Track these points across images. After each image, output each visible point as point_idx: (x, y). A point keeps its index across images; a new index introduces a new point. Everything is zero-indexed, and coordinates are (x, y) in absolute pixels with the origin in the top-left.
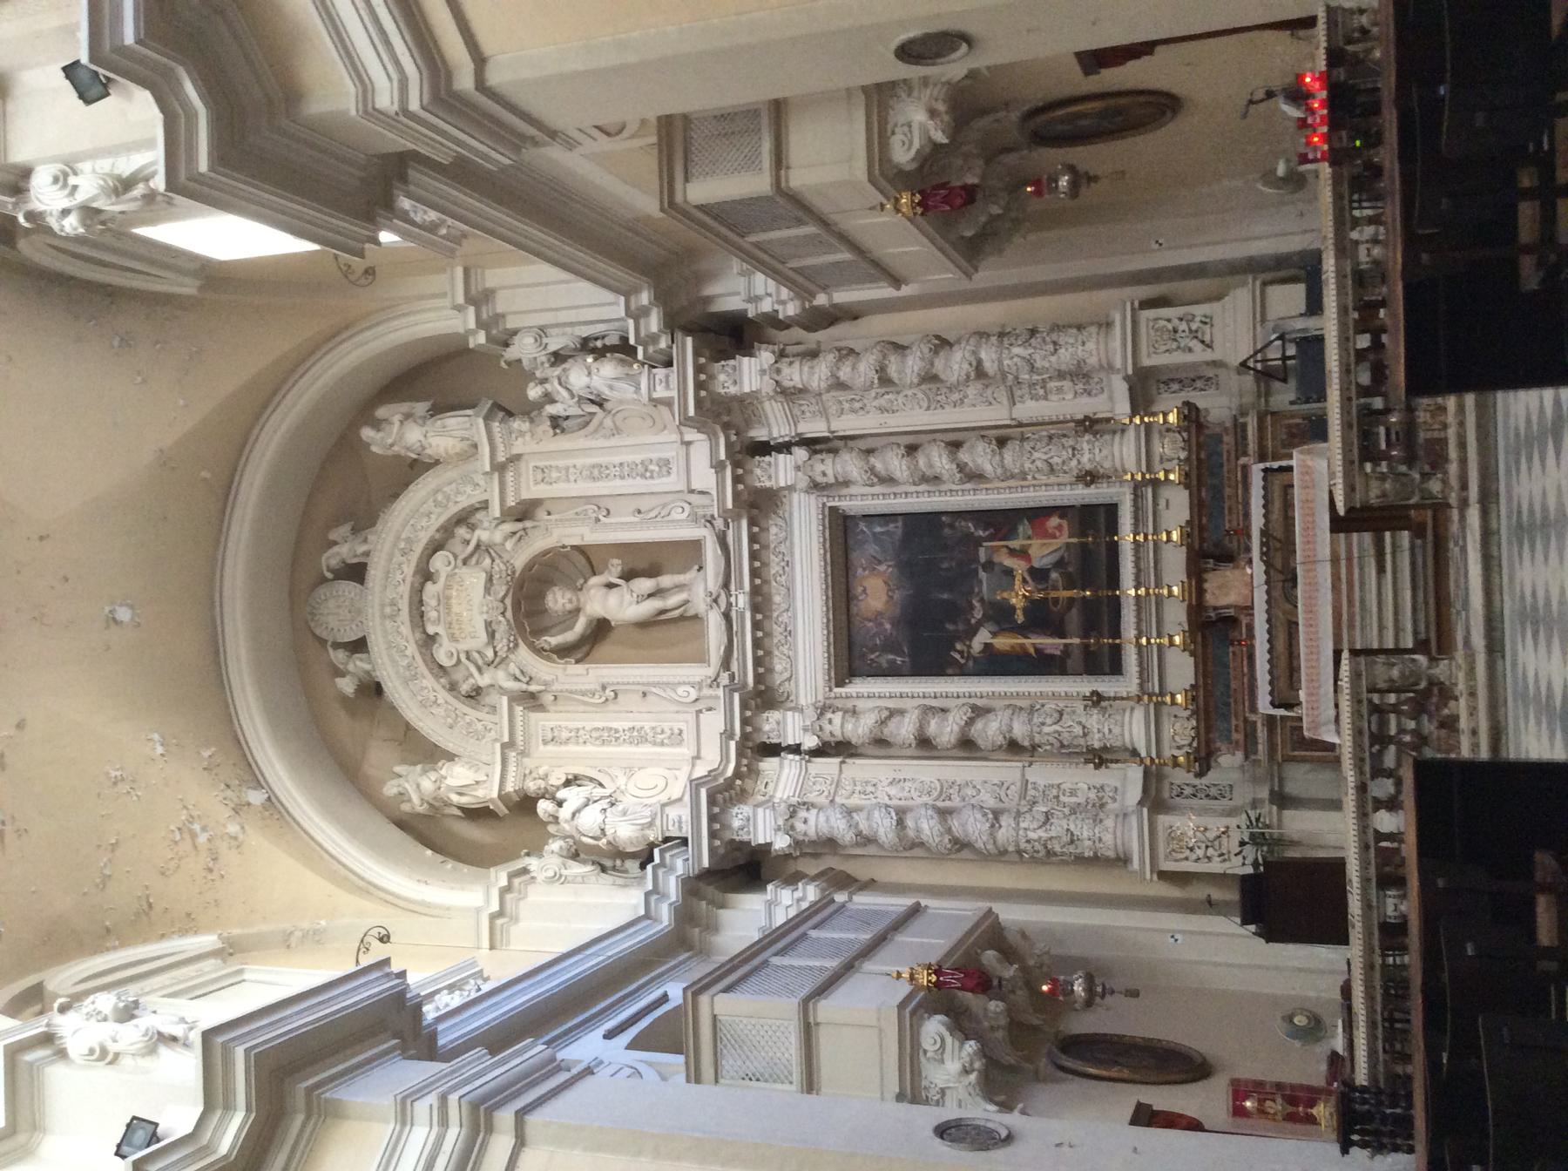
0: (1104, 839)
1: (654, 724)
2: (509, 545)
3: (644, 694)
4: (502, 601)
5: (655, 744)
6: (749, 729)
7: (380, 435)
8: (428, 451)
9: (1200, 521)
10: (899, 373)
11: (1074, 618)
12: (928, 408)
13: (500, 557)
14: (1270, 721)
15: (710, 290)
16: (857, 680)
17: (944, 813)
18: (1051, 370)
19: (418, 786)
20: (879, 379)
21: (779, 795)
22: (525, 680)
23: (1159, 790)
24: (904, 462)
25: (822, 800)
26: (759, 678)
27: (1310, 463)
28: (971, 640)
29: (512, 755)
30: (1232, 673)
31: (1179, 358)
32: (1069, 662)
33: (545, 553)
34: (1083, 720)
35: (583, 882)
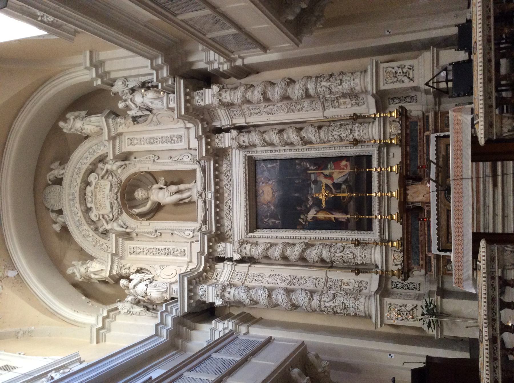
0: (359, 307)
1: (174, 247)
2: (119, 171)
3: (172, 234)
4: (116, 194)
5: (174, 255)
6: (211, 250)
7: (66, 125)
8: (84, 131)
9: (406, 162)
10: (272, 95)
11: (352, 206)
12: (287, 112)
13: (116, 176)
14: (438, 257)
15: (192, 59)
16: (259, 230)
17: (289, 292)
18: (339, 93)
19: (79, 270)
20: (264, 98)
21: (221, 280)
22: (125, 227)
23: (386, 284)
24: (277, 136)
25: (239, 283)
26: (217, 228)
27: (459, 118)
29: (116, 259)
30: (420, 233)
31: (398, 85)
32: (349, 225)
33: (135, 174)
34: (354, 251)
35: (140, 315)
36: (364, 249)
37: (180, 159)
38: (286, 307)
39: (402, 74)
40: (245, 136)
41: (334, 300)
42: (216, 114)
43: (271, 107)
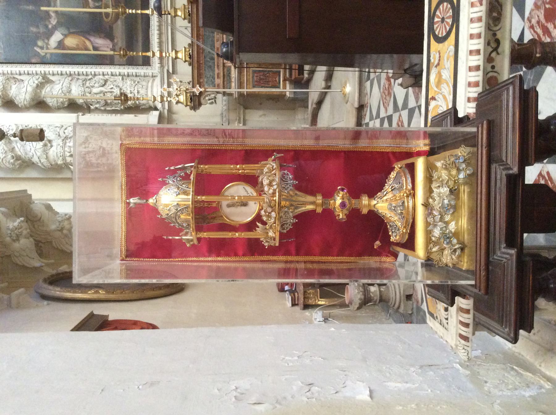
28: (48, 39)
34: (121, 86)
36: (136, 82)
38: (4, 162)
41: (87, 145)
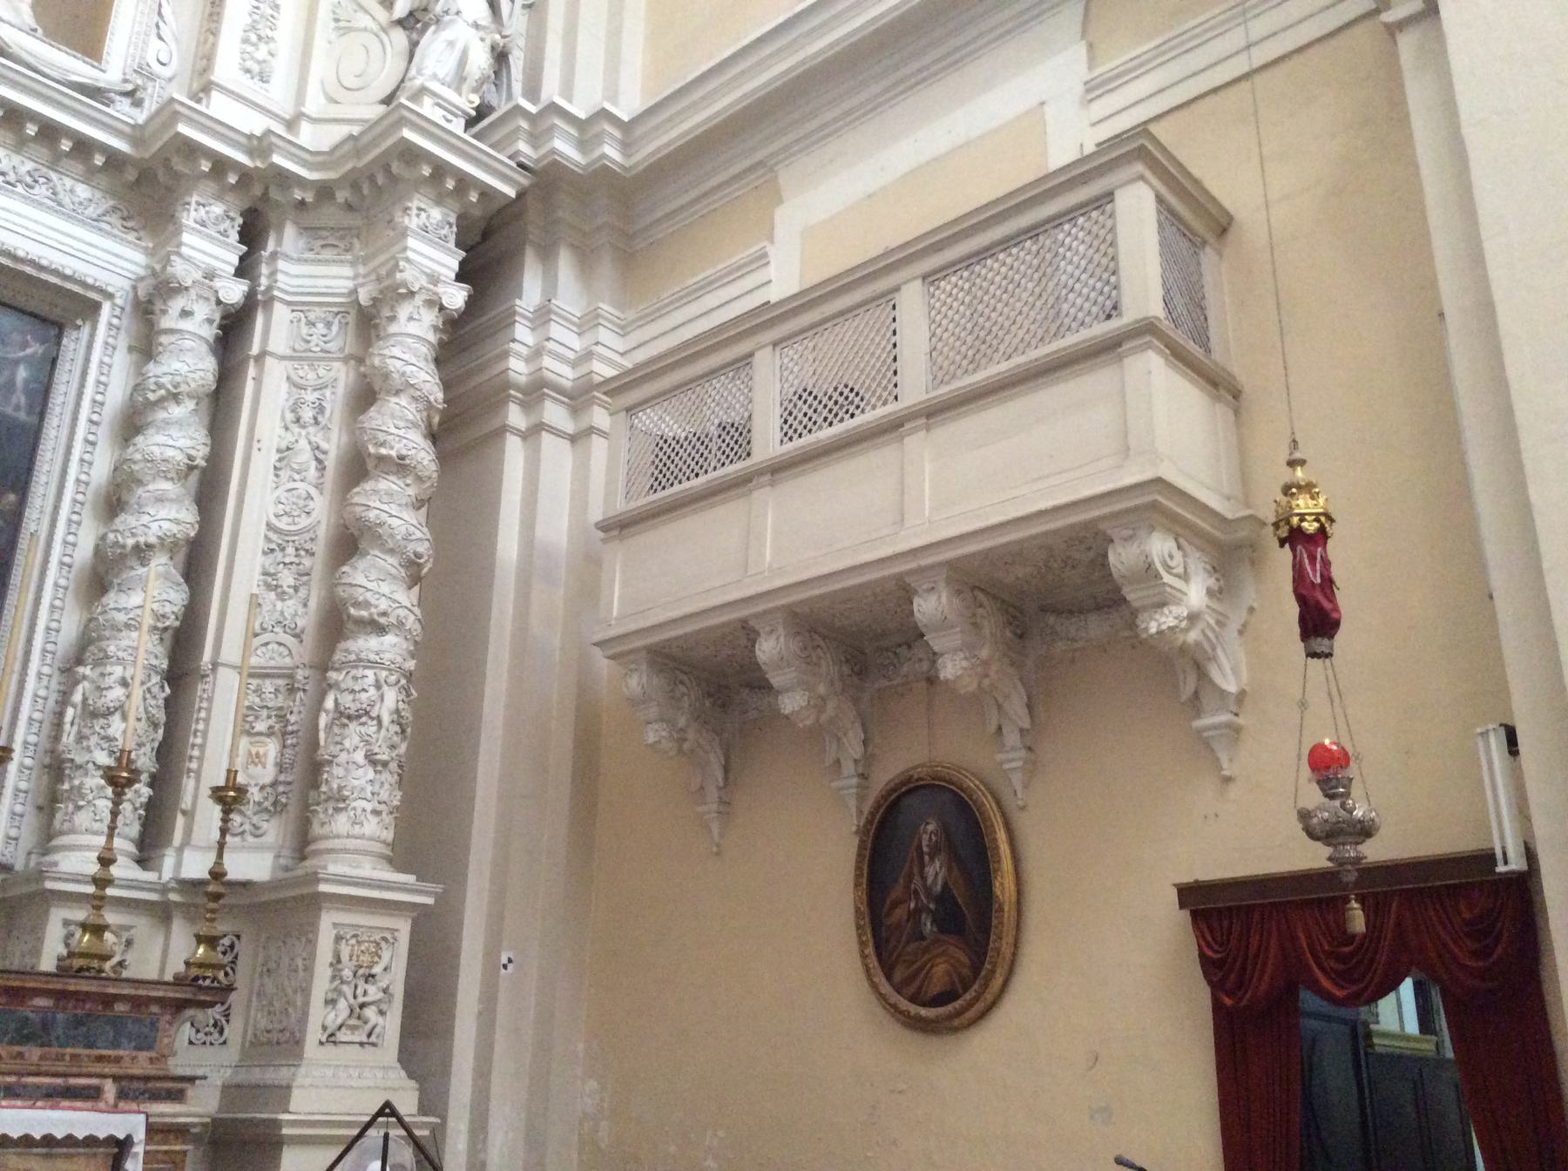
10: (390, 494)
12: (269, 526)
18: (334, 749)
20: (382, 459)
24: (180, 457)
37: (161, 24)
39: (361, 999)
40: (206, 326)
42: (327, 254)
43: (312, 472)
